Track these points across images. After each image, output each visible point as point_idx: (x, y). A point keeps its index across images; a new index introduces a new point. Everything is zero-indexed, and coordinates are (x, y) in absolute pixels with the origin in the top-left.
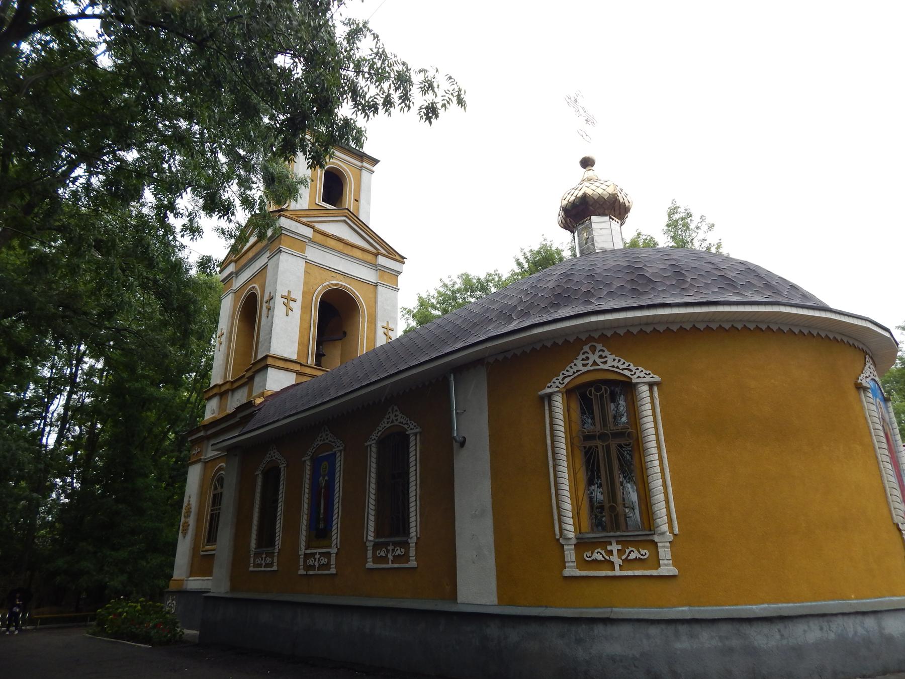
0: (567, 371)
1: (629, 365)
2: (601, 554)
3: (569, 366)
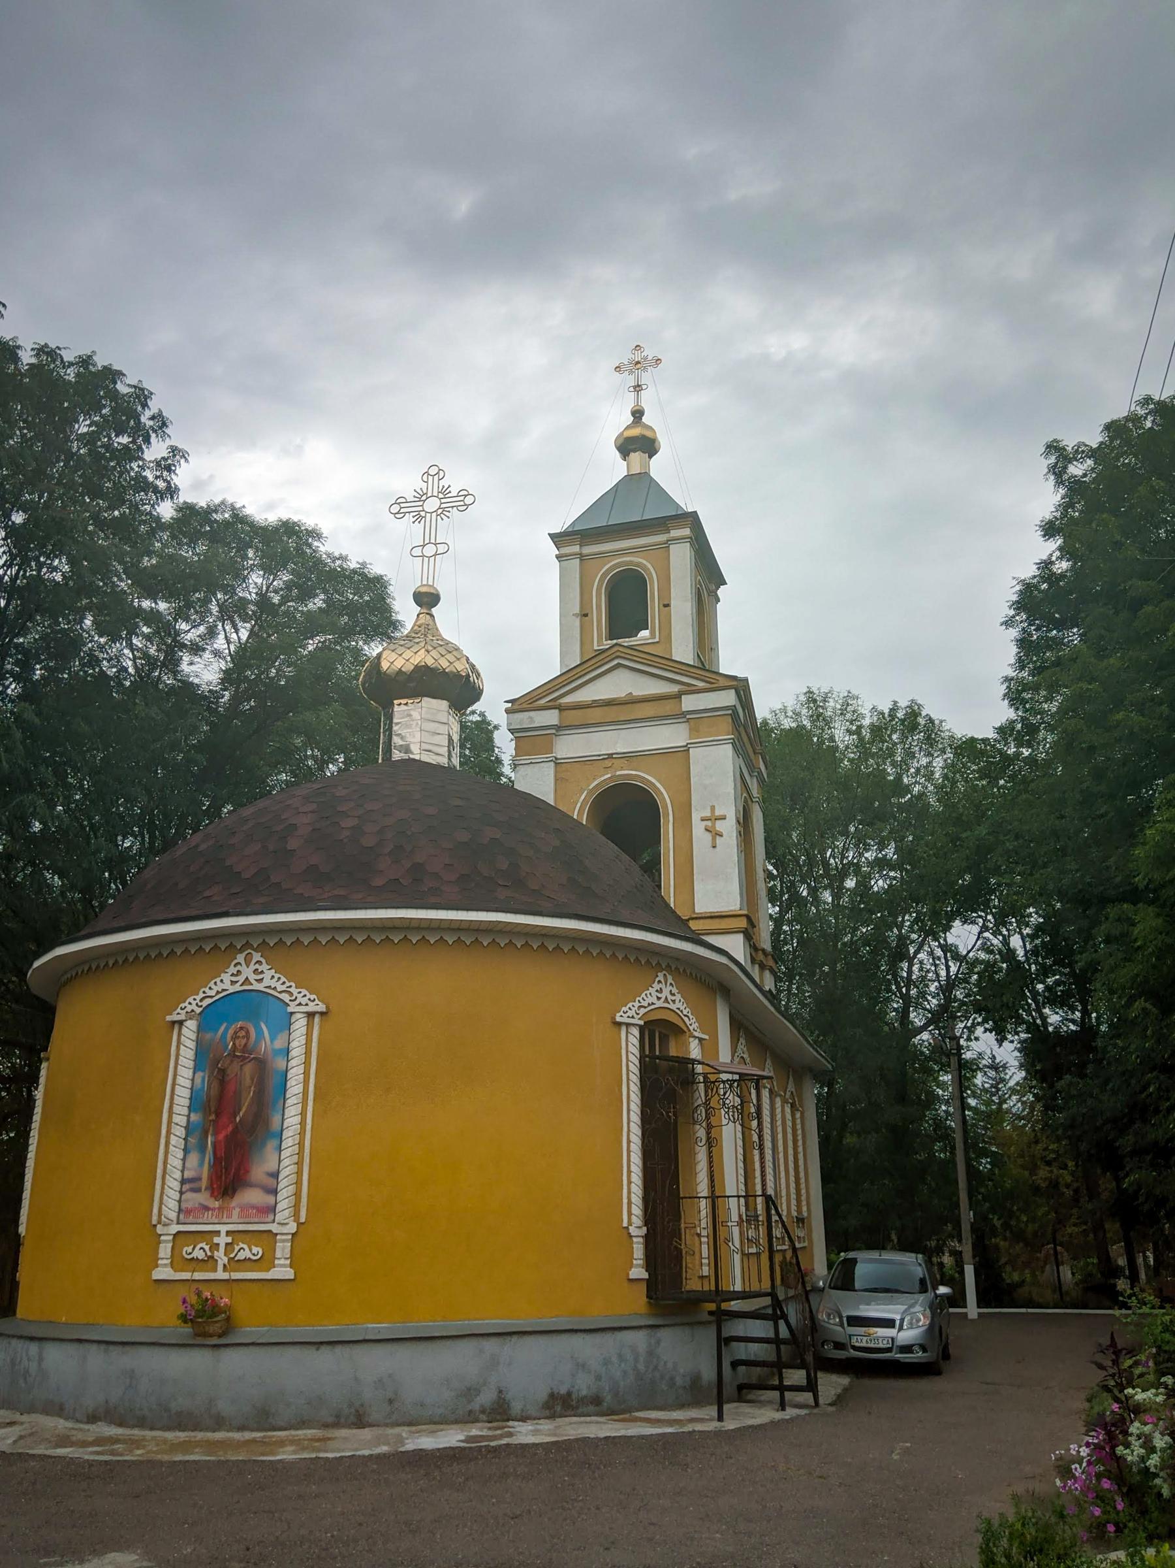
0: (210, 988)
1: (290, 986)
2: (204, 1251)
3: (214, 981)
